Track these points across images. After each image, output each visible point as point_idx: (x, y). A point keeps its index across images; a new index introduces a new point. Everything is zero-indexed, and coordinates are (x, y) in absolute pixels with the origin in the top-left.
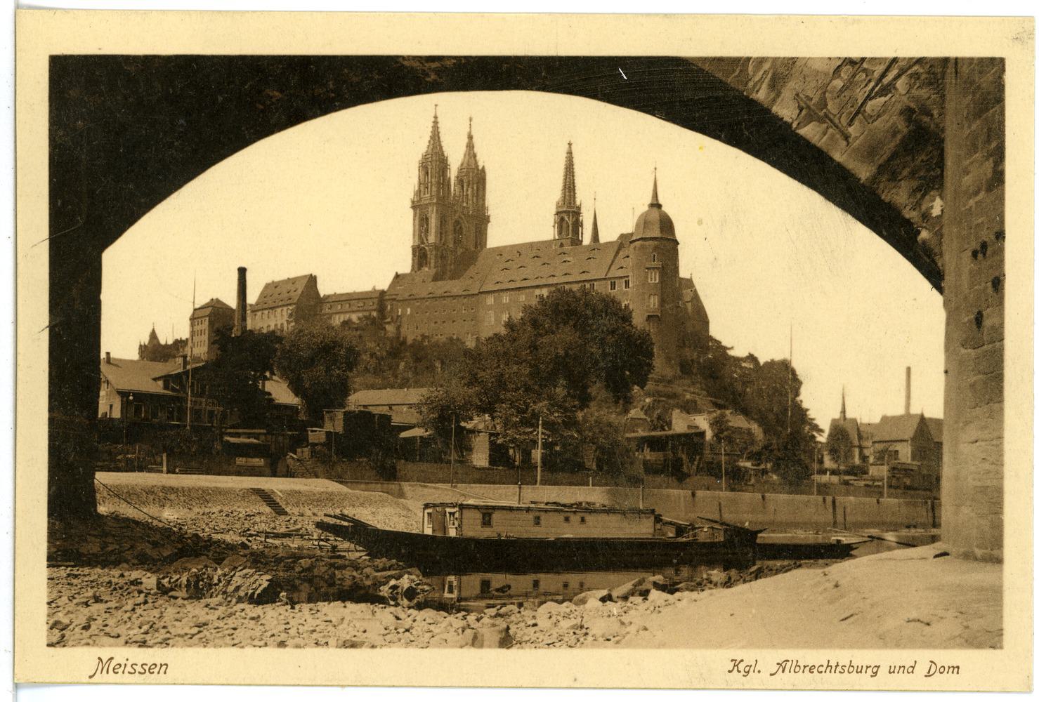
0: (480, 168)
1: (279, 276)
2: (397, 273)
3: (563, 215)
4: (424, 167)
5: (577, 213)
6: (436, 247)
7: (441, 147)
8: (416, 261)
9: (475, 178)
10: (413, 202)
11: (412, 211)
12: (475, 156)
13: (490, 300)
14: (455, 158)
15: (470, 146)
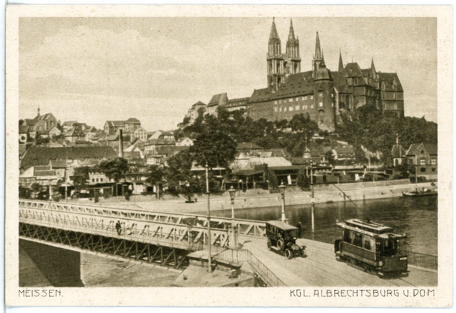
9: (294, 43)
13: (276, 102)
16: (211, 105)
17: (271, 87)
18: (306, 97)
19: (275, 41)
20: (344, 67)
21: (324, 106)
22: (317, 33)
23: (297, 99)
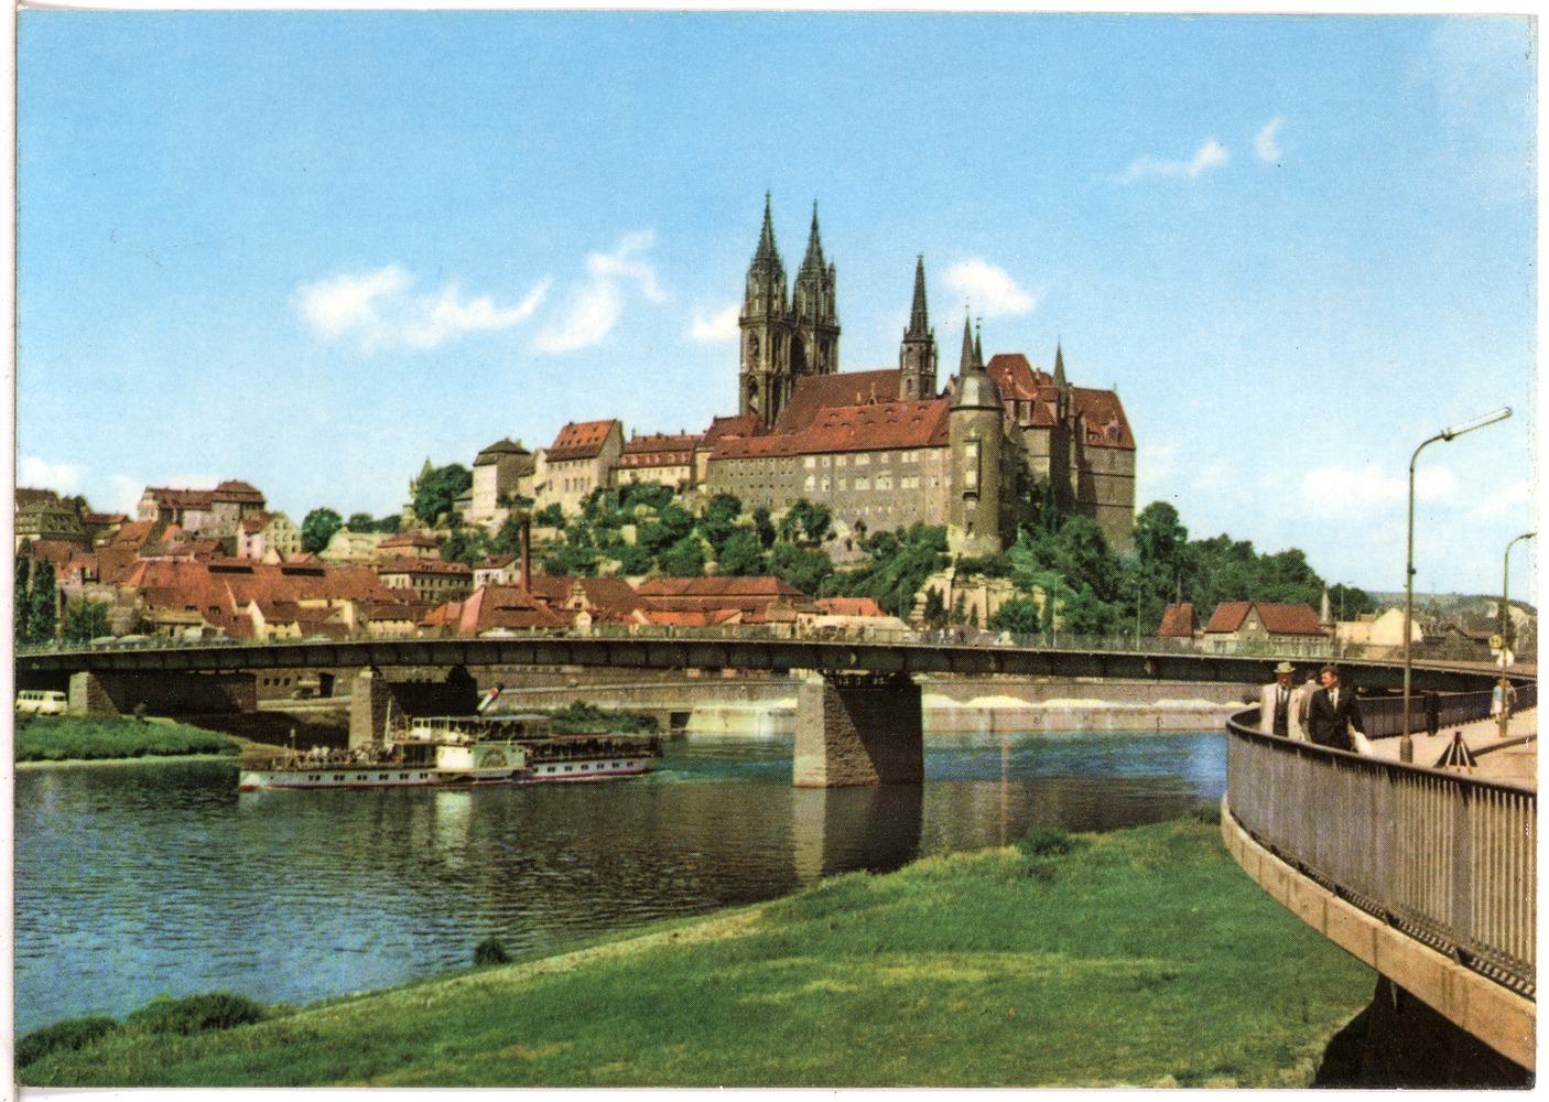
0: (827, 267)
1: (581, 417)
2: (716, 420)
3: (911, 345)
4: (753, 275)
5: (929, 341)
6: (768, 375)
7: (773, 253)
12: (819, 253)
13: (810, 462)
14: (792, 260)
15: (815, 239)
16: (561, 454)
18: (914, 456)
19: (767, 264)
20: (986, 361)
21: (979, 480)
22: (920, 258)
23: (885, 457)
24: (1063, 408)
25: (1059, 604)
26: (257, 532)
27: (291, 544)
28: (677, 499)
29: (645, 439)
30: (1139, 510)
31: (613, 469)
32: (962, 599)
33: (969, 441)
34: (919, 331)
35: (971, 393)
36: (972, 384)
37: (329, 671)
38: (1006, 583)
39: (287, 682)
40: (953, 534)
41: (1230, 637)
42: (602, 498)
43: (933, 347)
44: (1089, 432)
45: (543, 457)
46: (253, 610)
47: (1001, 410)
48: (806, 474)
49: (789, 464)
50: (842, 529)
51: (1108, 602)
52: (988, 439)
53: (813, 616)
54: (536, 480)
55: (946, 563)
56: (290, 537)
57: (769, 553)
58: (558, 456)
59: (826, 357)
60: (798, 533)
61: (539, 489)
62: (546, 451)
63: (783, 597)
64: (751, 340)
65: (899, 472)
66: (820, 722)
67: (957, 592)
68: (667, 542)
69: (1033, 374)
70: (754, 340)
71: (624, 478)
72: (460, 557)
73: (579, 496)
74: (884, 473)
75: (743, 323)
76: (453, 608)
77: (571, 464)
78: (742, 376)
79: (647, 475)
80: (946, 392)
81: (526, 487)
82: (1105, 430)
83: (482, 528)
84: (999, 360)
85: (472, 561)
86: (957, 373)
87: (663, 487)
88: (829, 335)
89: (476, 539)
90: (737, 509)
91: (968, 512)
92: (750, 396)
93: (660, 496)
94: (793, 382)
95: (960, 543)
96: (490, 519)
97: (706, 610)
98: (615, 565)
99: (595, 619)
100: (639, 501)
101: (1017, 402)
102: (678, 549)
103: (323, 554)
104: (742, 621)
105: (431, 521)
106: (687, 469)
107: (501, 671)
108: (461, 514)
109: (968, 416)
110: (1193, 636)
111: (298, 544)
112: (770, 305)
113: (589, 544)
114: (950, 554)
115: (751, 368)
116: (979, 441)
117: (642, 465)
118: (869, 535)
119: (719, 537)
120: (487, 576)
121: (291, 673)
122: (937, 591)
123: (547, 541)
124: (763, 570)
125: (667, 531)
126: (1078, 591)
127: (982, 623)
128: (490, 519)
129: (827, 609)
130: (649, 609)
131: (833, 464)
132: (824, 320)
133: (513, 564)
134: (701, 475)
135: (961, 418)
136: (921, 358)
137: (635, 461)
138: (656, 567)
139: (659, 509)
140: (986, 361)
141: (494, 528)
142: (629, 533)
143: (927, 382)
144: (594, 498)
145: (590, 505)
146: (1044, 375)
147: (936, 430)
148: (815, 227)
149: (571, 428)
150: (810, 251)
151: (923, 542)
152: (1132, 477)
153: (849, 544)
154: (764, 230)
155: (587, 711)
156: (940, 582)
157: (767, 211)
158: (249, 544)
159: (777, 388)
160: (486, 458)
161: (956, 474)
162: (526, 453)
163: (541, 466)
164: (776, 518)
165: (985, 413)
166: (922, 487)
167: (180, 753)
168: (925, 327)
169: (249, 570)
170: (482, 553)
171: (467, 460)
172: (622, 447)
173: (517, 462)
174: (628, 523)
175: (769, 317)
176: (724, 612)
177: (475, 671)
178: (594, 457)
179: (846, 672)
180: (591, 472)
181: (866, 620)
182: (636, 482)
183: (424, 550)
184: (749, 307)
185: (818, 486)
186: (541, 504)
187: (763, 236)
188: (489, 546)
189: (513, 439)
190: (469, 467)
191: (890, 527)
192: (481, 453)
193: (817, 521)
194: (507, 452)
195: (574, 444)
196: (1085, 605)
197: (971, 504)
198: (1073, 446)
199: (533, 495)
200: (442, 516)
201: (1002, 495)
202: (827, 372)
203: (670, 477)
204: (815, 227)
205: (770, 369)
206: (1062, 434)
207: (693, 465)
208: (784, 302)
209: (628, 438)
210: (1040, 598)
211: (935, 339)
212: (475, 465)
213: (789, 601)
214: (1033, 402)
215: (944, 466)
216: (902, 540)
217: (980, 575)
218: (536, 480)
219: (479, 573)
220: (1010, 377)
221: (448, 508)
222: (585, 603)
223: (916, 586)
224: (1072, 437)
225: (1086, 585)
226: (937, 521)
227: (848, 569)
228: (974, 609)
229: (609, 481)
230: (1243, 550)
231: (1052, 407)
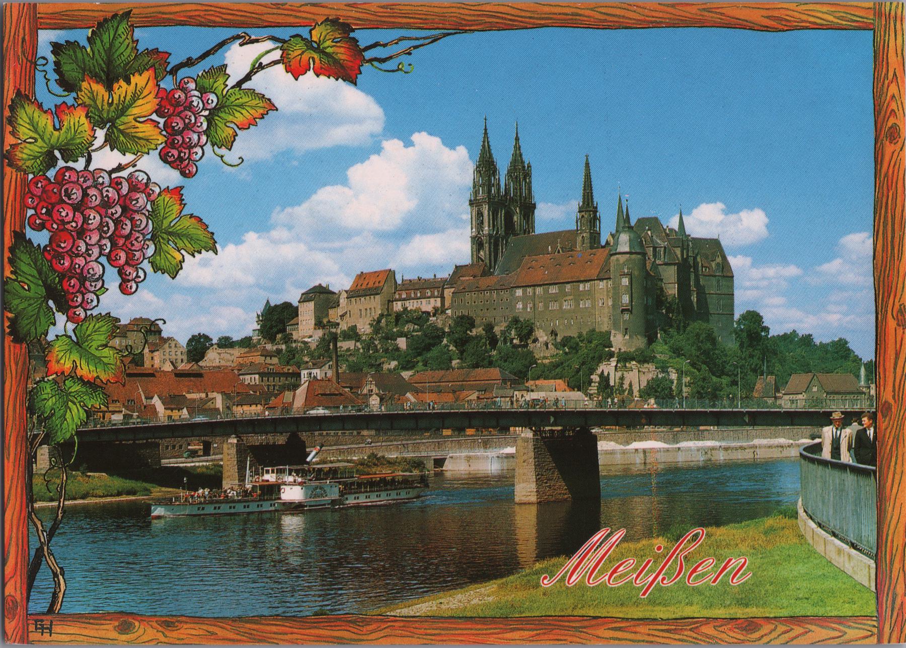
2: (456, 267)
3: (583, 213)
5: (595, 210)
6: (490, 236)
8: (475, 249)
10: (470, 201)
11: (469, 207)
12: (521, 155)
13: (519, 292)
15: (517, 147)
17: (479, 258)
18: (588, 285)
21: (631, 301)
22: (587, 156)
23: (568, 287)
24: (685, 252)
25: (686, 379)
26: (158, 350)
27: (180, 357)
28: (432, 319)
29: (410, 281)
30: (737, 316)
31: (390, 301)
32: (622, 378)
33: (624, 275)
34: (588, 204)
35: (624, 243)
36: (624, 237)
37: (207, 439)
38: (651, 366)
39: (181, 447)
40: (614, 336)
41: (800, 396)
42: (383, 321)
43: (598, 214)
44: (702, 267)
45: (344, 295)
46: (156, 401)
47: (644, 254)
48: (518, 299)
49: (505, 295)
50: (542, 336)
51: (719, 377)
52: (636, 273)
53: (525, 393)
54: (340, 311)
55: (611, 355)
56: (179, 353)
57: (494, 353)
58: (353, 294)
59: (527, 222)
60: (513, 339)
61: (342, 316)
62: (346, 291)
63: (504, 381)
64: (478, 214)
65: (579, 297)
66: (532, 460)
67: (619, 374)
68: (428, 348)
69: (665, 230)
70: (480, 214)
71: (398, 307)
72: (291, 362)
73: (368, 320)
74: (567, 298)
75: (471, 203)
76: (288, 395)
77: (363, 299)
78: (473, 238)
79: (411, 305)
80: (607, 243)
81: (334, 315)
82: (713, 264)
83: (305, 343)
84: (642, 222)
85: (299, 365)
86: (614, 232)
87: (424, 312)
88: (529, 209)
89: (302, 350)
90: (472, 325)
91: (625, 321)
92: (478, 251)
93: (421, 318)
94: (507, 241)
95: (619, 341)
96: (310, 337)
97: (454, 392)
98: (394, 364)
99: (381, 399)
100: (407, 322)
101: (655, 248)
102: (434, 352)
103: (201, 363)
104: (478, 398)
105: (272, 339)
106: (439, 299)
107: (321, 435)
108: (292, 334)
109: (622, 259)
110: (776, 398)
111: (185, 357)
112: (489, 191)
113: (377, 351)
114: (613, 349)
115: (479, 232)
116: (630, 275)
117: (409, 298)
118: (559, 339)
119: (462, 343)
120: (310, 374)
121: (182, 441)
122: (606, 374)
123: (348, 350)
124: (491, 364)
125: (427, 341)
126: (699, 370)
127: (636, 393)
128: (310, 337)
129: (534, 388)
130: (416, 392)
131: (534, 293)
132: (526, 198)
133: (327, 366)
134: (447, 304)
135: (618, 260)
136: (590, 222)
137: (404, 296)
138: (420, 364)
139: (421, 326)
140: (633, 222)
141: (313, 342)
142: (402, 343)
143: (595, 237)
144: (379, 321)
145: (376, 325)
146: (671, 230)
147: (602, 269)
148: (517, 139)
149: (361, 276)
150: (514, 155)
151: (594, 342)
152: (733, 295)
153: (546, 344)
154: (484, 142)
155: (378, 459)
156: (608, 368)
157: (486, 130)
158: (152, 358)
159: (496, 245)
160: (306, 297)
161: (616, 298)
162: (334, 293)
163: (343, 301)
164: (497, 330)
165: (633, 256)
166: (594, 307)
167: (111, 496)
168: (592, 202)
169: (152, 375)
170: (306, 359)
171: (293, 298)
172: (396, 288)
173: (328, 299)
174: (402, 337)
175: (489, 199)
176: (465, 393)
177: (304, 436)
178: (378, 294)
179: (547, 428)
180: (375, 305)
181: (559, 394)
182: (405, 309)
183: (268, 358)
184: (476, 193)
185: (525, 307)
186: (344, 326)
187: (484, 146)
188: (311, 355)
189: (324, 285)
190: (295, 303)
191: (573, 333)
192: (303, 294)
193: (527, 332)
194: (321, 293)
195: (364, 287)
196: (704, 379)
197: (627, 316)
198: (692, 276)
199: (339, 321)
200: (279, 336)
201: (647, 309)
202: (529, 232)
203: (427, 306)
204: (517, 139)
205: (491, 233)
206: (685, 269)
207: (442, 297)
208: (499, 189)
209: (399, 282)
210: (674, 376)
211: (599, 209)
212: (299, 302)
213: (509, 383)
214: (665, 248)
215: (608, 292)
216: (582, 341)
217: (634, 363)
218: (340, 311)
219: (304, 373)
220: (649, 232)
221: (283, 330)
222: (375, 390)
223: (592, 371)
224: (692, 270)
225: (704, 367)
226: (605, 328)
227: (546, 361)
228: (631, 385)
229: (388, 309)
230: (807, 340)
231: (678, 251)
